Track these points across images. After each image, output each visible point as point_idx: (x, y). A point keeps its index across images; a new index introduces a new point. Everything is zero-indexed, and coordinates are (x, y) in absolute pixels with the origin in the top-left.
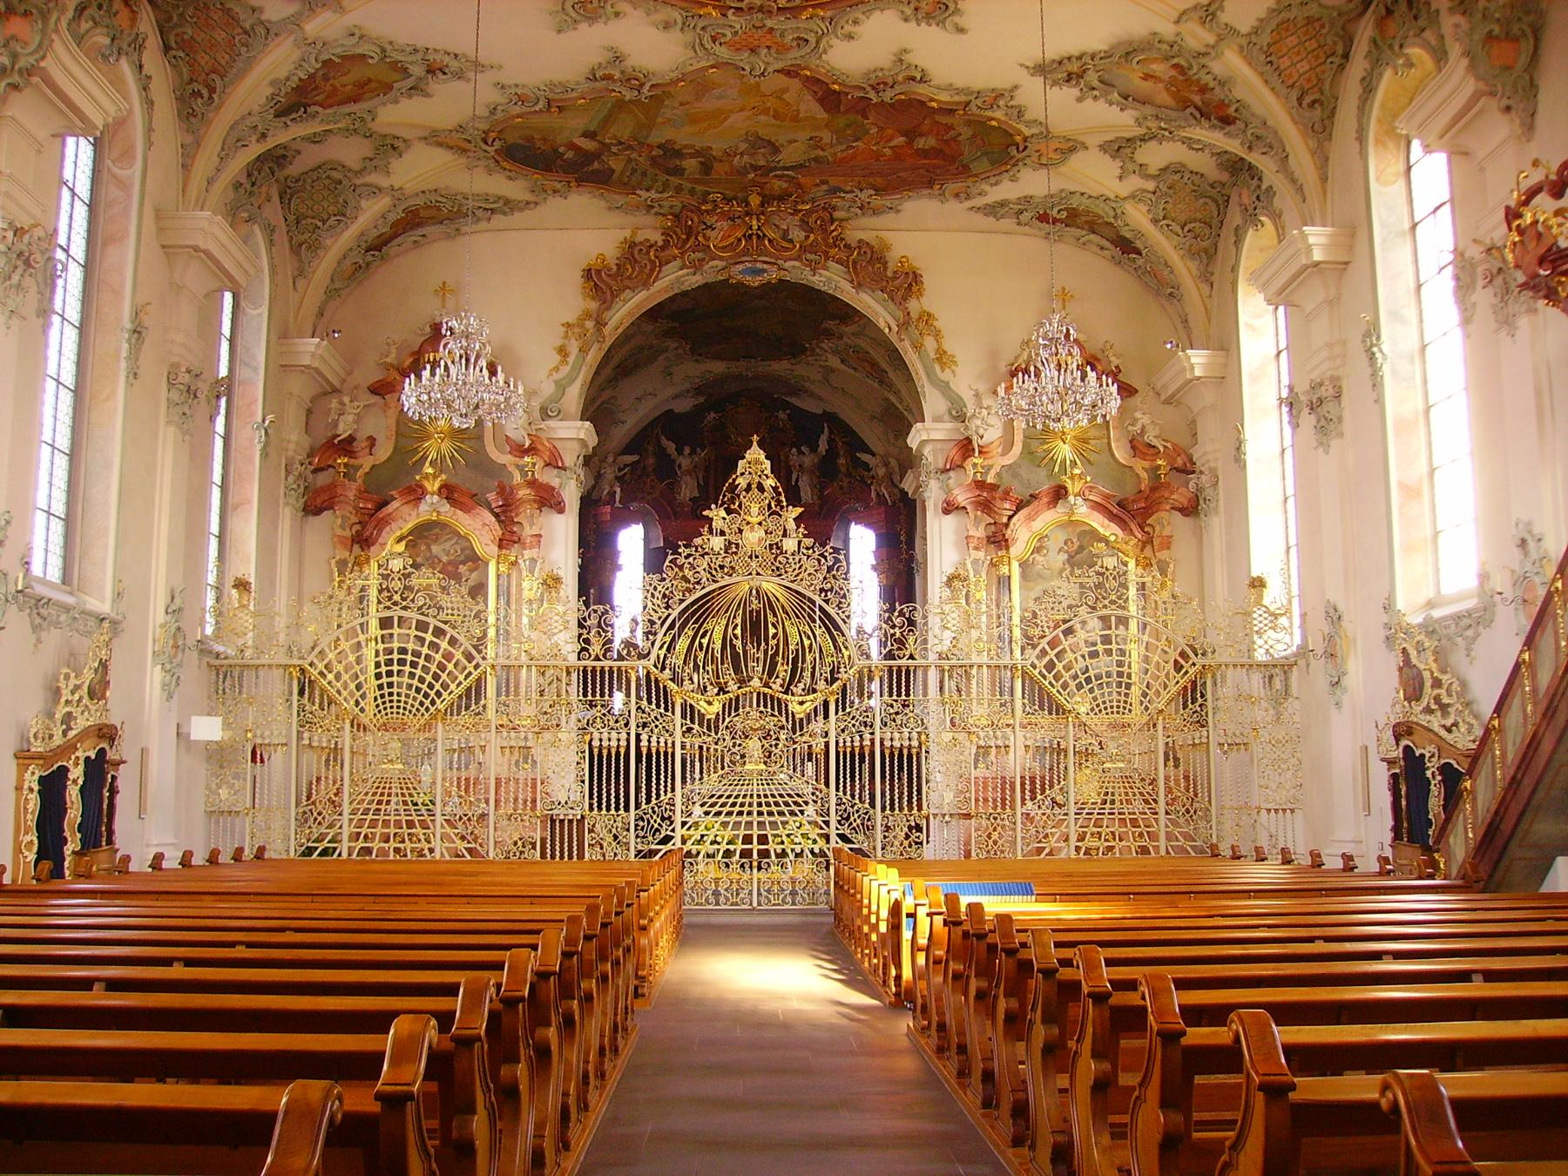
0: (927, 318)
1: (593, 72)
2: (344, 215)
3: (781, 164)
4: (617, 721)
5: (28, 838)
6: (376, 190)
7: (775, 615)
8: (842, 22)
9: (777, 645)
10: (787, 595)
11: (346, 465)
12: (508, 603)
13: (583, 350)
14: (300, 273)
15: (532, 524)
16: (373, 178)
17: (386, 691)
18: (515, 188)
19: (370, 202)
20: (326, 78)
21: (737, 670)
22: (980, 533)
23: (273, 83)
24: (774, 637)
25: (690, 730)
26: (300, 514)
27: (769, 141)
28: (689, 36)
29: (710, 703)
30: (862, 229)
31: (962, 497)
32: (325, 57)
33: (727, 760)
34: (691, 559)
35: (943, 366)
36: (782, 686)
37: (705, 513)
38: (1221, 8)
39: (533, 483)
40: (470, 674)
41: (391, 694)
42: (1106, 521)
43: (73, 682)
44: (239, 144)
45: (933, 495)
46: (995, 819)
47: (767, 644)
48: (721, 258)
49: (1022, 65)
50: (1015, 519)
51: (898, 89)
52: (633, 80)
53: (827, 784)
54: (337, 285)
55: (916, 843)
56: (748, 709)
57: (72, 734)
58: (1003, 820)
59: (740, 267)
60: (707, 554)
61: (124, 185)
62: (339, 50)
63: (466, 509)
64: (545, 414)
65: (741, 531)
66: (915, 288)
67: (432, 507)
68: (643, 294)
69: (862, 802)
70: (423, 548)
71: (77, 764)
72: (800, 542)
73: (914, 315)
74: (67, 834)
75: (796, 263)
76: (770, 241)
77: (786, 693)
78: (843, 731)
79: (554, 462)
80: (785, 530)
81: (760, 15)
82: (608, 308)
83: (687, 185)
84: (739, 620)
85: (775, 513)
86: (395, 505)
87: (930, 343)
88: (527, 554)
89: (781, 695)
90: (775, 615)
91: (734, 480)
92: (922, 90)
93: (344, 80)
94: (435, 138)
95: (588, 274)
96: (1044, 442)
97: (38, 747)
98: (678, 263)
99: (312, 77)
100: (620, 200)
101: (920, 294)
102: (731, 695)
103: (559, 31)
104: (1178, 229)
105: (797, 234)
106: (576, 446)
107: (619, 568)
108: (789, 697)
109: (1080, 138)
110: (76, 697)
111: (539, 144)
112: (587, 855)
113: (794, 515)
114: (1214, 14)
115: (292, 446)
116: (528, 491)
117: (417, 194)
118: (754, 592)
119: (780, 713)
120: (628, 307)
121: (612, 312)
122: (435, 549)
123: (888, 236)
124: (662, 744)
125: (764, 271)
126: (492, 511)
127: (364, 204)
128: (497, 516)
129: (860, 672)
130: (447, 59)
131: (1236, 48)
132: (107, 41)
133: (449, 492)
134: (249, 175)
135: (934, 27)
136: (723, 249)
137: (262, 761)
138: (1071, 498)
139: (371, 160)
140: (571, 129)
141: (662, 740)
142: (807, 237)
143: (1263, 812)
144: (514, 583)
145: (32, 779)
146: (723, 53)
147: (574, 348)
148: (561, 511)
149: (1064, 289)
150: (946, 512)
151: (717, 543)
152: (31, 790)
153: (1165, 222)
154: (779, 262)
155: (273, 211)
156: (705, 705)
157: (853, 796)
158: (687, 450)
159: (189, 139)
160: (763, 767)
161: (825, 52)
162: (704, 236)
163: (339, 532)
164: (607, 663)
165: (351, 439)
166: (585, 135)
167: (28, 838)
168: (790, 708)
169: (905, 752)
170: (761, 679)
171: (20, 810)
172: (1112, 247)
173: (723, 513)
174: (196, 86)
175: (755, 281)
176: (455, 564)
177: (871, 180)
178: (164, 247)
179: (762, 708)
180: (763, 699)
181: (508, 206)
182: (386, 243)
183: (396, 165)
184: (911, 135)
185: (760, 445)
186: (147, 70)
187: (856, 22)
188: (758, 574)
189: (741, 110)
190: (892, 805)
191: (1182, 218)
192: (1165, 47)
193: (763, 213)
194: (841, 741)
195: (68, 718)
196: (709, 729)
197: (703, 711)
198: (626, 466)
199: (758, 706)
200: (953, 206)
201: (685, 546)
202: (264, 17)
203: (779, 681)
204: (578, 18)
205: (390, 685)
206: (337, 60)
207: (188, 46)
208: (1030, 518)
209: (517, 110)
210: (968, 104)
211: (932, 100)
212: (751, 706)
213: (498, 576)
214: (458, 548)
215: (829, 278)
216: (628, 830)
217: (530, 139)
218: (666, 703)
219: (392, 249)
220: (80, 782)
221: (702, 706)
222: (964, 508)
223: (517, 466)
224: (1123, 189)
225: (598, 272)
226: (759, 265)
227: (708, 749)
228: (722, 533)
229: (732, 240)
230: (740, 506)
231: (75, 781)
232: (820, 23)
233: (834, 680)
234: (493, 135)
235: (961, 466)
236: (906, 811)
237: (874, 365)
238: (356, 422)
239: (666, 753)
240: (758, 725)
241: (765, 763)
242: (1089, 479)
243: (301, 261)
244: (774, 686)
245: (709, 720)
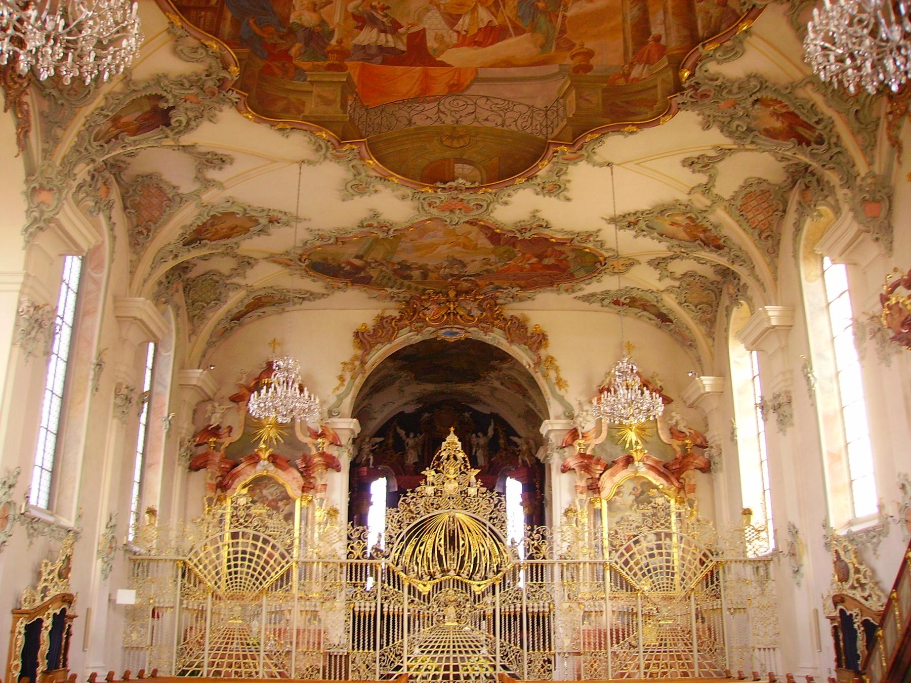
0: (550, 360)
1: (362, 222)
2: (219, 300)
3: (467, 274)
4: (369, 596)
5: (16, 662)
6: (238, 287)
8: (502, 195)
9: (465, 551)
10: (471, 521)
11: (215, 442)
12: (306, 524)
13: (353, 378)
14: (193, 332)
15: (322, 478)
16: (236, 280)
17: (233, 576)
18: (315, 285)
19: (234, 293)
20: (212, 225)
21: (441, 564)
22: (583, 483)
23: (182, 227)
24: (463, 545)
25: (413, 601)
26: (187, 470)
27: (460, 261)
28: (416, 203)
29: (425, 585)
30: (513, 310)
31: (572, 463)
32: (212, 213)
33: (435, 619)
34: (414, 499)
35: (560, 387)
36: (468, 575)
37: (423, 473)
38: (713, 186)
39: (323, 454)
40: (283, 567)
41: (236, 578)
42: (657, 477)
43: (50, 568)
44: (163, 260)
45: (555, 461)
46: (595, 655)
47: (459, 550)
48: (432, 326)
49: (602, 218)
50: (603, 476)
51: (533, 232)
52: (385, 227)
53: (494, 634)
54: (214, 340)
55: (548, 671)
56: (447, 589)
57: (47, 599)
58: (600, 656)
59: (443, 331)
60: (423, 496)
61: (96, 282)
62: (220, 210)
63: (284, 469)
64: (331, 414)
65: (444, 483)
66: (543, 343)
67: (264, 467)
68: (388, 346)
69: (516, 645)
70: (258, 491)
71: (48, 618)
73: (543, 358)
74: (39, 660)
75: (476, 329)
76: (461, 316)
77: (470, 579)
78: (504, 602)
79: (335, 442)
80: (470, 483)
81: (456, 192)
82: (368, 354)
83: (414, 285)
84: (442, 536)
85: (464, 473)
86: (242, 466)
87: (552, 374)
88: (319, 495)
89: (466, 581)
90: (464, 533)
92: (546, 232)
93: (223, 226)
94: (272, 258)
95: (357, 334)
96: (619, 430)
97: (26, 607)
98: (408, 329)
99: (204, 224)
100: (376, 293)
101: (546, 346)
102: (437, 581)
103: (344, 200)
104: (693, 308)
105: (476, 312)
106: (348, 433)
107: (371, 504)
109: (636, 258)
110: (51, 577)
111: (330, 262)
112: (350, 677)
113: (475, 474)
114: (709, 189)
115: (184, 431)
116: (320, 459)
117: (261, 289)
118: (451, 519)
119: (466, 590)
120: (379, 354)
121: (371, 355)
122: (265, 492)
123: (529, 314)
124: (396, 610)
125: (457, 333)
126: (298, 470)
127: (231, 294)
128: (301, 473)
129: (514, 567)
130: (280, 215)
131: (723, 207)
132: (93, 204)
133: (274, 459)
134: (167, 277)
135: (553, 198)
136: (434, 321)
137: (158, 617)
138: (636, 463)
139: (236, 270)
140: (348, 254)
141: (396, 607)
142: (482, 314)
143: (756, 650)
144: (310, 512)
145: (21, 626)
146: (435, 212)
147: (348, 376)
148: (339, 471)
149: (629, 342)
150: (563, 471)
151: (430, 490)
152: (20, 633)
153: (686, 304)
154: (466, 328)
155: (179, 298)
156: (422, 586)
157: (510, 641)
158: (412, 435)
159: (135, 257)
160: (456, 624)
161: (492, 212)
162: (423, 314)
163: (209, 481)
164: (364, 561)
165: (218, 428)
166: (357, 257)
167: (16, 662)
169: (541, 615)
170: (455, 570)
171: (12, 645)
172: (656, 319)
173: (433, 473)
174: (140, 229)
175: (452, 339)
176: (276, 501)
177: (518, 282)
178: (117, 317)
179: (455, 589)
180: (457, 583)
181: (312, 296)
182: (242, 316)
183: (250, 273)
184: (541, 257)
186: (113, 220)
187: (509, 196)
189: (444, 244)
190: (533, 646)
191: (696, 302)
192: (683, 207)
193: (456, 301)
194: (503, 608)
195: (45, 590)
196: (424, 600)
197: (420, 590)
198: (376, 444)
199: (454, 587)
200: (565, 297)
202: (180, 191)
203: (466, 572)
204: (354, 193)
205: (236, 573)
206: (219, 215)
207: (137, 207)
208: (613, 475)
209: (318, 243)
210: (572, 240)
211: (552, 238)
212: (449, 587)
213: (301, 508)
214: (278, 491)
215: (494, 337)
216: (375, 662)
217: (326, 259)
218: (399, 585)
219: (246, 319)
220: (50, 628)
221: (420, 587)
222: (574, 469)
223: (314, 444)
224: (662, 286)
225: (363, 333)
226: (454, 330)
228: (433, 484)
229: (438, 316)
230: (443, 468)
231: (46, 628)
232: (489, 196)
233: (498, 572)
234: (305, 257)
236: (542, 651)
237: (520, 386)
238: (222, 418)
239: (398, 616)
240: (453, 599)
241: (458, 621)
242: (646, 452)
243: (193, 325)
244: (463, 575)
245: (424, 596)
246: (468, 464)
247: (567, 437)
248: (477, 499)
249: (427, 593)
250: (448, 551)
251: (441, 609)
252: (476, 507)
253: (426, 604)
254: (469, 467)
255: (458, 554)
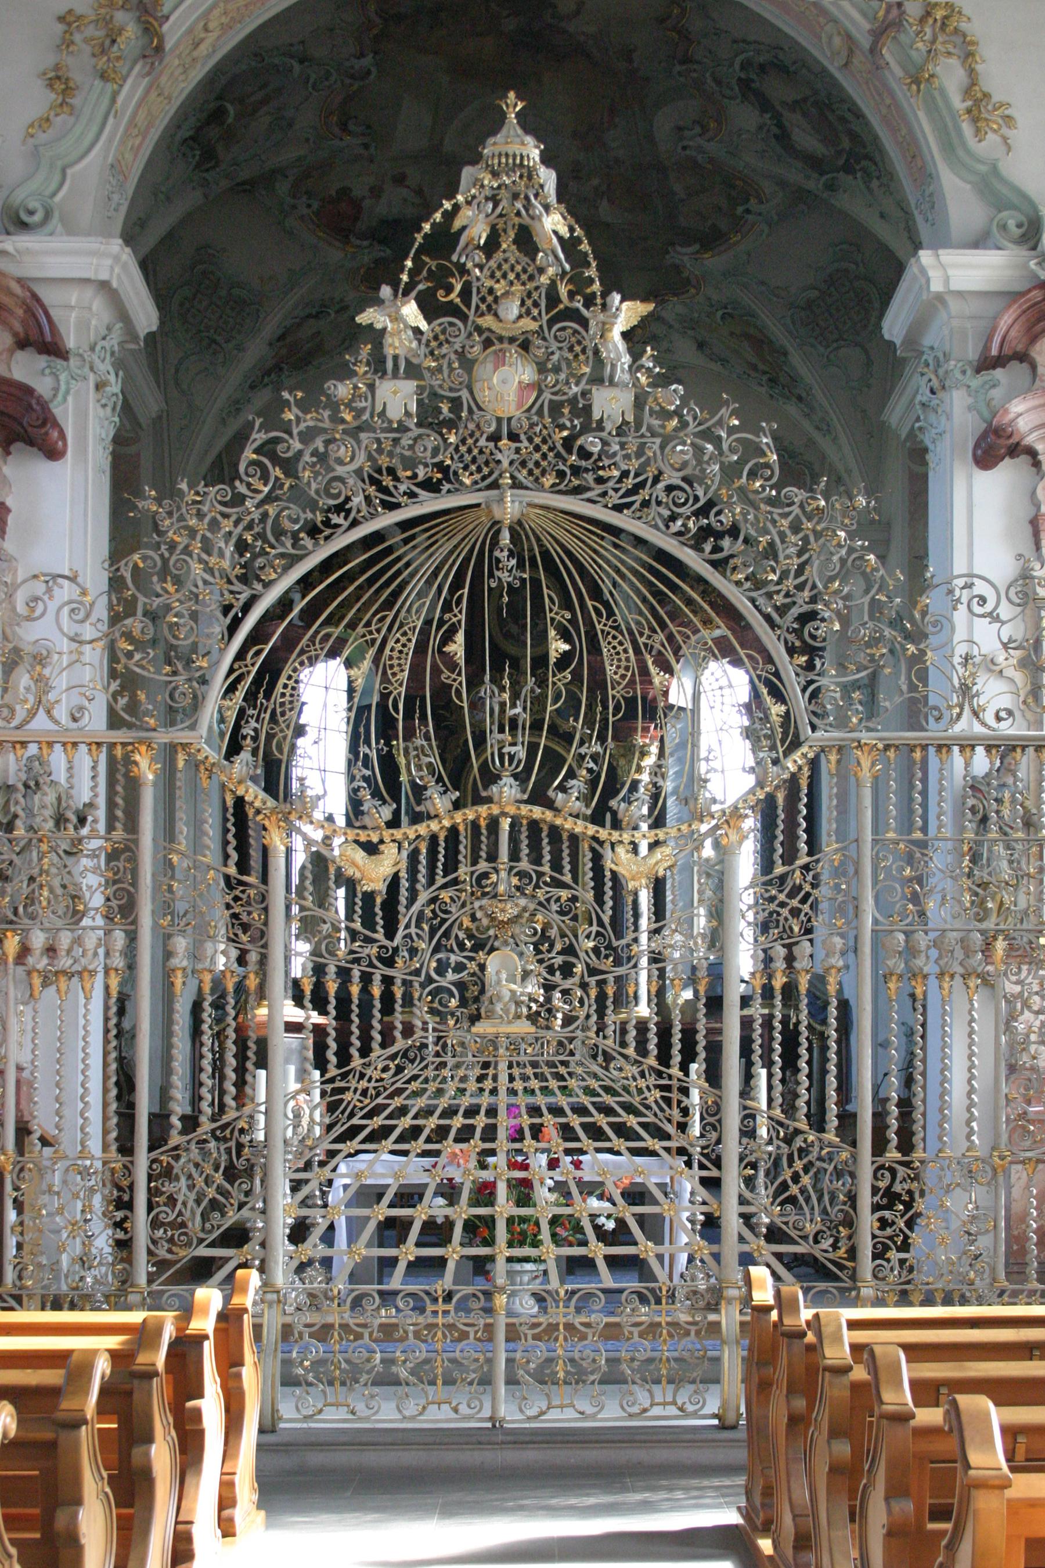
7: (567, 604)
29: (371, 849)
34: (319, 444)
37: (368, 316)
47: (542, 682)
56: (483, 866)
65: (468, 364)
72: (639, 402)
77: (597, 819)
80: (599, 362)
84: (460, 616)
85: (572, 315)
89: (580, 827)
91: (450, 216)
102: (434, 826)
106: (100, 312)
108: (603, 834)
118: (505, 539)
168: (608, 864)
179: (524, 865)
185: (528, 123)
188: (516, 485)
199: (514, 856)
201: (301, 404)
203: (577, 786)
212: (492, 857)
227: (366, 979)
235: (1023, 357)
245: (369, 897)
246: (592, 272)
247: (1006, 320)
248: (633, 444)
249: (381, 887)
250: (487, 687)
251: (453, 958)
252: (630, 482)
253: (380, 935)
254: (597, 287)
255: (539, 702)
